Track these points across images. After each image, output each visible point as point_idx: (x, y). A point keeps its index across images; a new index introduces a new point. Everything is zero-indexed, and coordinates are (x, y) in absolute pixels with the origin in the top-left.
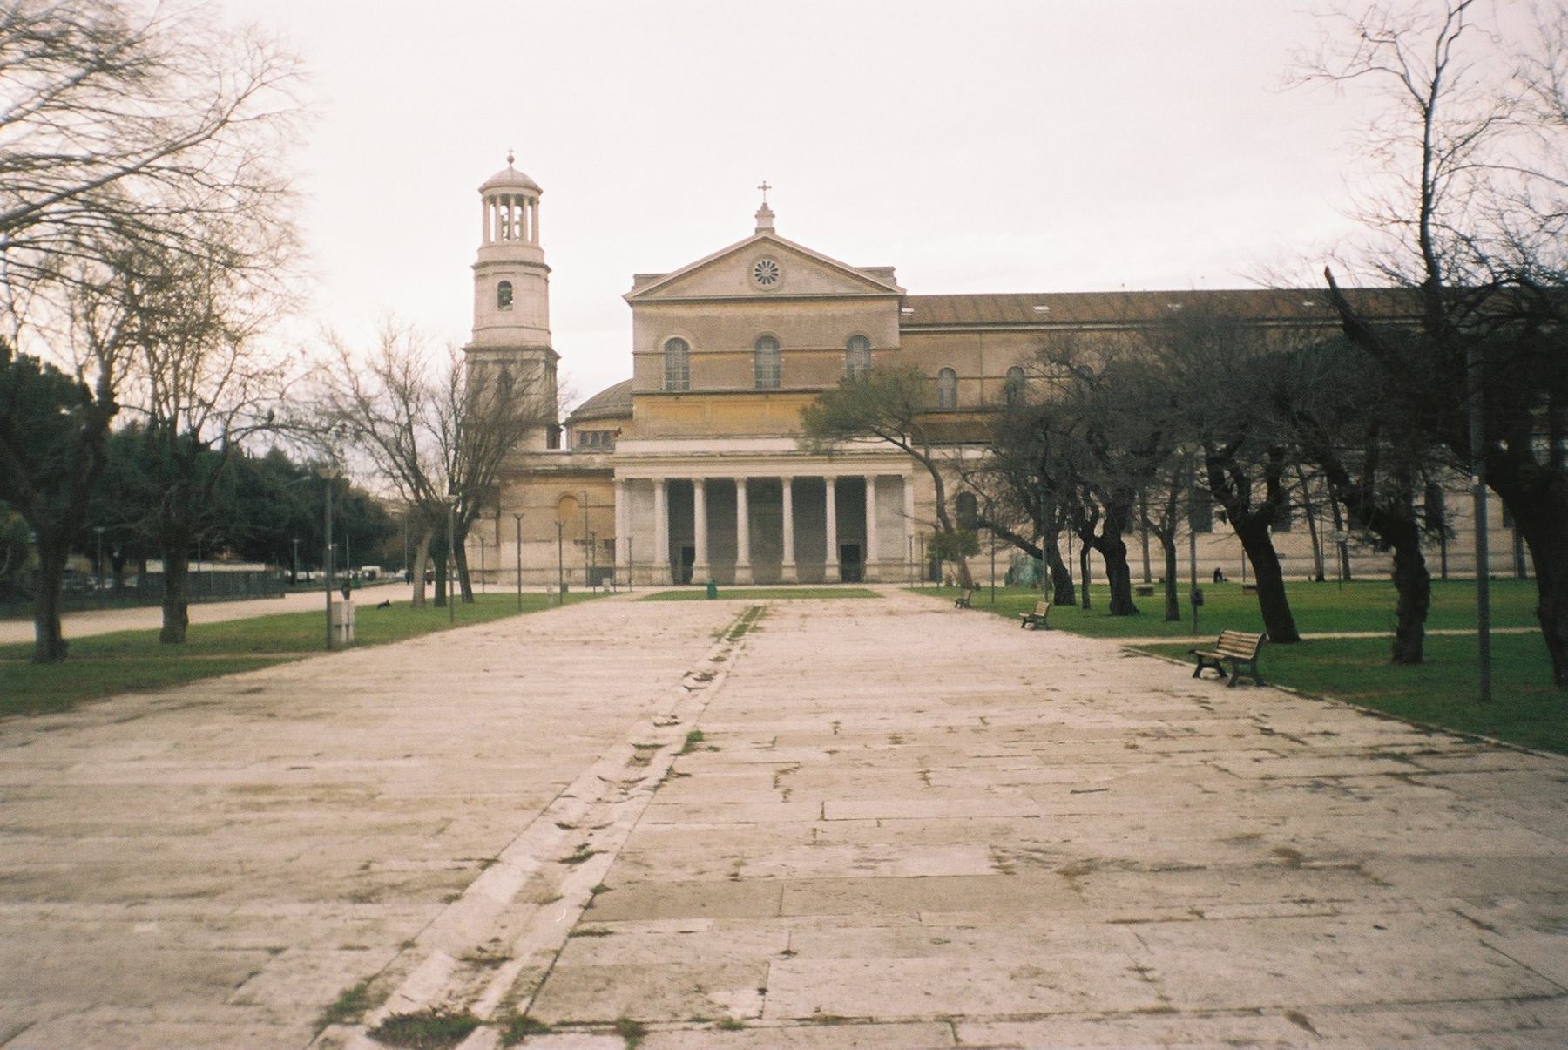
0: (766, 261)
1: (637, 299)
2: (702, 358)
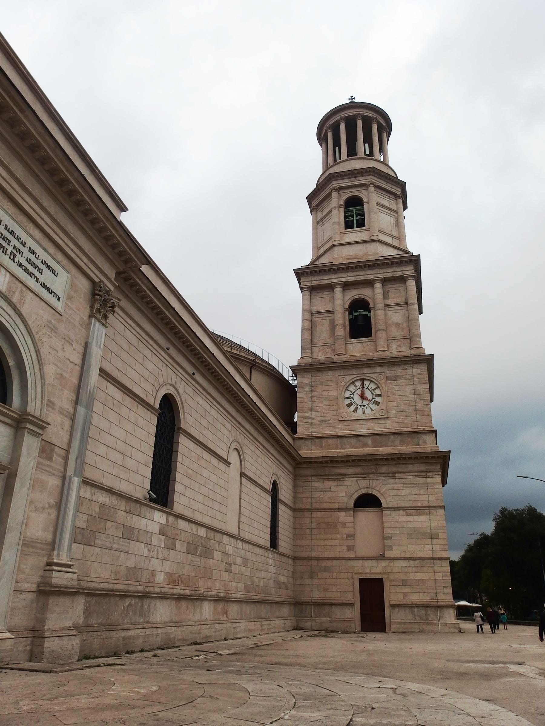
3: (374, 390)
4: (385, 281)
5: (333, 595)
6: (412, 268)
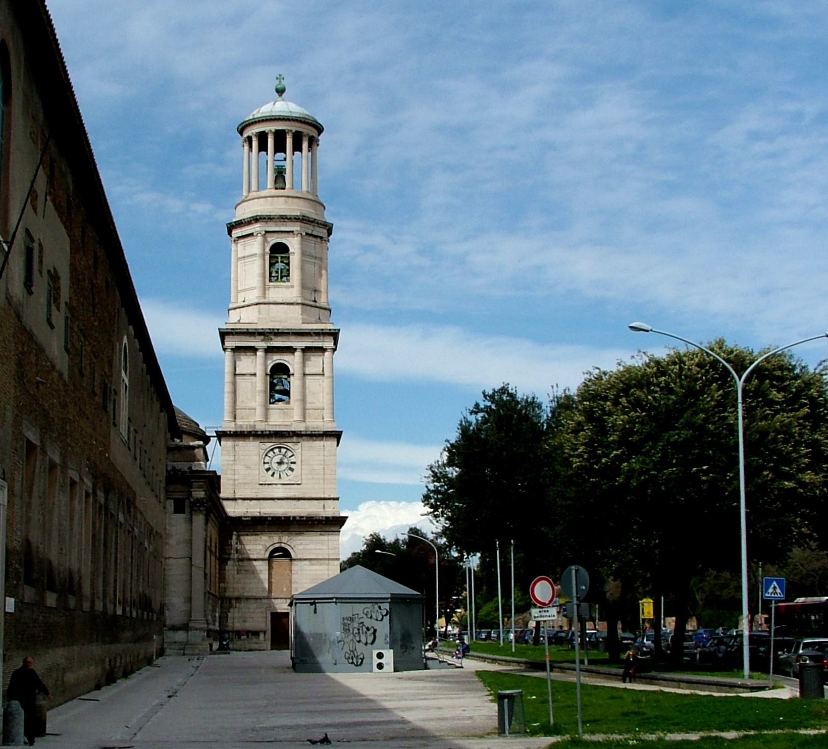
3: (290, 457)
4: (306, 350)
5: (250, 625)
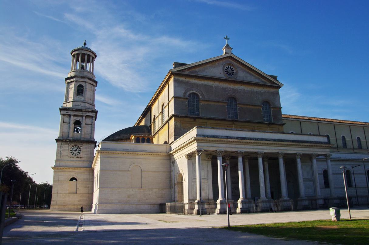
0: (229, 66)
1: (177, 72)
2: (206, 103)
6: (95, 114)
